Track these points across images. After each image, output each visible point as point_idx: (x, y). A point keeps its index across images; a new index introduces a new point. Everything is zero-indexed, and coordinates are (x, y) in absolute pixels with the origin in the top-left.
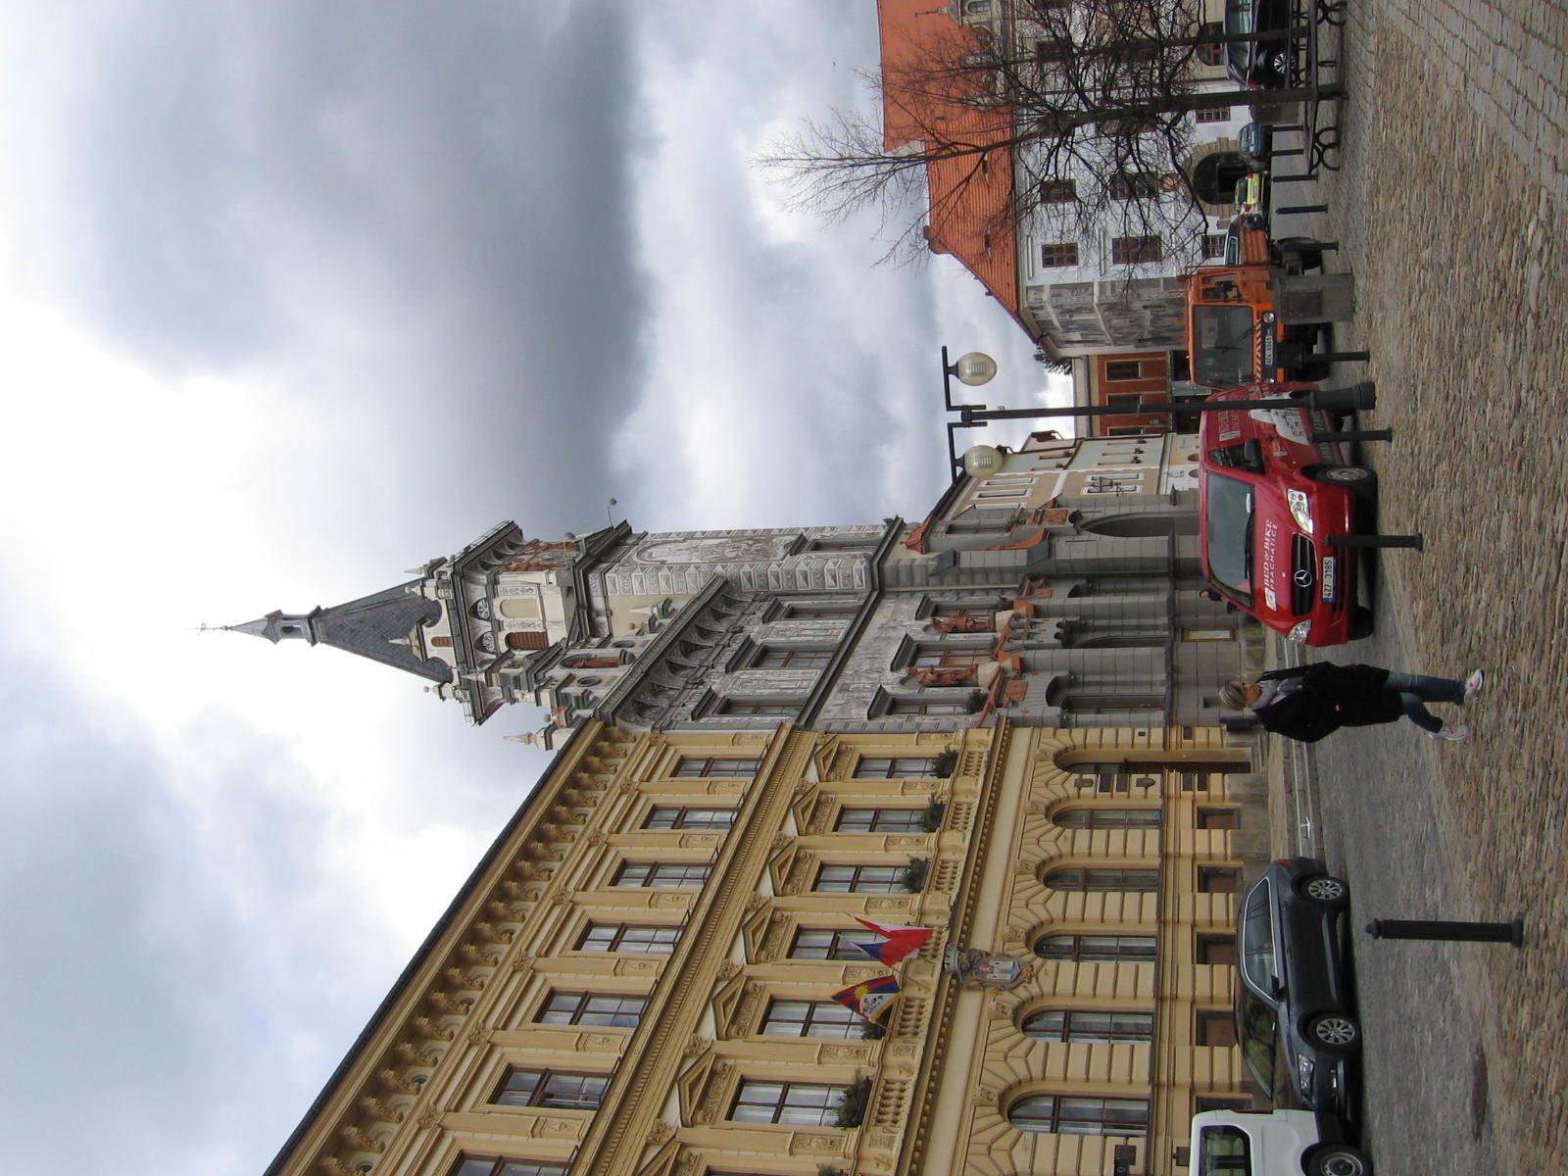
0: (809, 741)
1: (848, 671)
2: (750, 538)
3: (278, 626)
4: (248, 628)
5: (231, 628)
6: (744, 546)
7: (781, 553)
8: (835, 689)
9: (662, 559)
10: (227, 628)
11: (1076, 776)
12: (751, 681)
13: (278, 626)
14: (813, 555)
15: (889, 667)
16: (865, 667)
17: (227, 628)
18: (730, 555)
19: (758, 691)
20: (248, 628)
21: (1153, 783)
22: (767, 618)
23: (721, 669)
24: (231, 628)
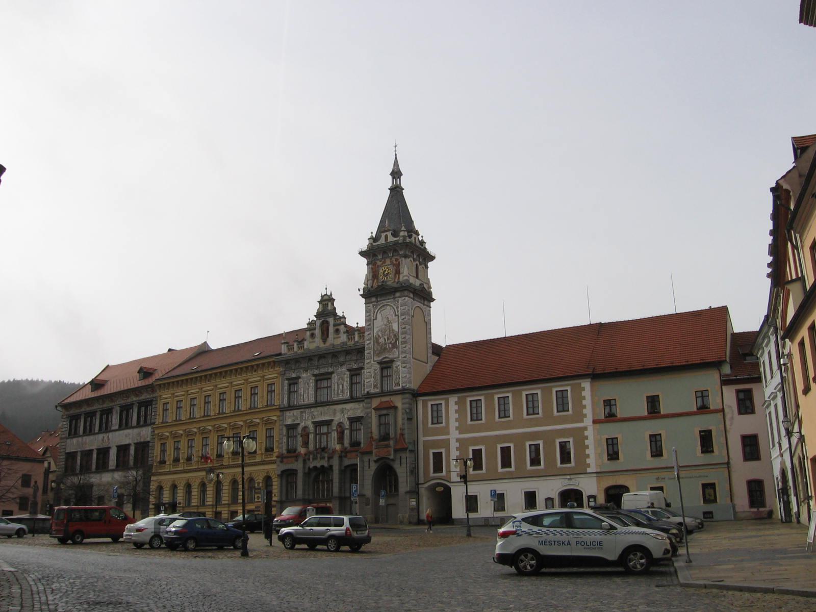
0: (278, 413)
1: (313, 410)
2: (397, 339)
3: (396, 174)
4: (396, 163)
5: (396, 157)
6: (389, 341)
7: (381, 358)
8: (302, 410)
9: (379, 316)
10: (396, 155)
11: (261, 481)
12: (308, 384)
13: (396, 174)
14: (378, 370)
15: (315, 420)
16: (315, 413)
17: (396, 155)
18: (382, 340)
19: (302, 389)
20: (396, 163)
21: (258, 499)
22: (349, 370)
23: (316, 372)
24: (396, 157)
